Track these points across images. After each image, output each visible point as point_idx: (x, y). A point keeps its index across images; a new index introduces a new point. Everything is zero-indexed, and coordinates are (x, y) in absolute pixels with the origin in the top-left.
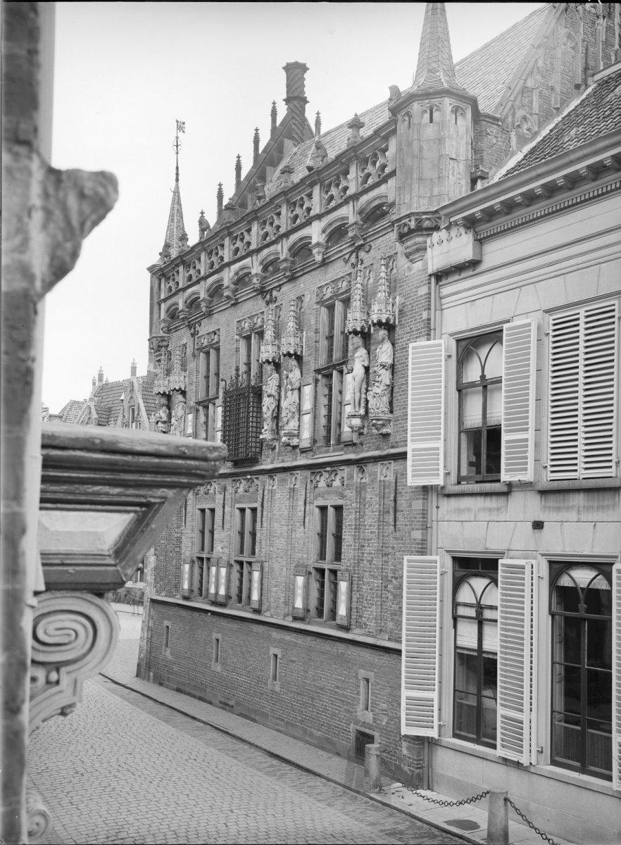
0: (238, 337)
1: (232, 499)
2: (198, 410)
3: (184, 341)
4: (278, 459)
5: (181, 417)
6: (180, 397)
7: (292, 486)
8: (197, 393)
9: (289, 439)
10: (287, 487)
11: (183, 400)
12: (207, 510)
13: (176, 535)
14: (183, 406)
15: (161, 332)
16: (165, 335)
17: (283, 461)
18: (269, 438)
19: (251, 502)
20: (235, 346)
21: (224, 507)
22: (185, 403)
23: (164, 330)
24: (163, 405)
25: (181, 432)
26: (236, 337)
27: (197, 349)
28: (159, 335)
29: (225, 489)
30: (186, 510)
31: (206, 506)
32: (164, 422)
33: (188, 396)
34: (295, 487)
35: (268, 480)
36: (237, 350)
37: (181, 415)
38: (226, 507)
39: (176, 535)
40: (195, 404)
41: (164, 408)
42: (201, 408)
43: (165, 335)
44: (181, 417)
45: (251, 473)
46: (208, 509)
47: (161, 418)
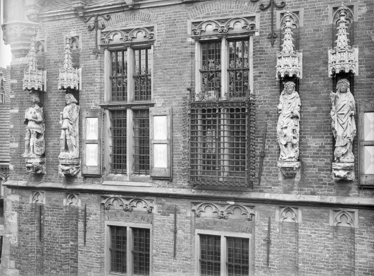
0: (193, 41)
1: (191, 223)
2: (104, 114)
3: (73, 34)
4: (301, 190)
5: (76, 120)
6: (72, 98)
7: (335, 224)
8: (101, 94)
9: (348, 173)
10: (326, 224)
11: (76, 101)
12: (128, 229)
13: (63, 251)
14: (78, 108)
15: (26, 18)
16: (31, 22)
17: (313, 194)
18: (297, 166)
19: (232, 231)
20: (189, 50)
21: (175, 232)
22: (78, 104)
23: (33, 17)
24: (36, 102)
25: (75, 137)
26: (190, 40)
27: (101, 46)
28: (24, 22)
29: (176, 211)
30: (85, 225)
31: (129, 224)
32: (38, 123)
33: (82, 97)
34: (340, 225)
35: (277, 212)
36: (192, 54)
37: (75, 119)
38: (179, 232)
39: (63, 251)
40: (100, 108)
41: (37, 107)
42: (107, 112)
43: (31, 22)
44: (76, 120)
45: (235, 200)
46: (130, 227)
47: (36, 118)
